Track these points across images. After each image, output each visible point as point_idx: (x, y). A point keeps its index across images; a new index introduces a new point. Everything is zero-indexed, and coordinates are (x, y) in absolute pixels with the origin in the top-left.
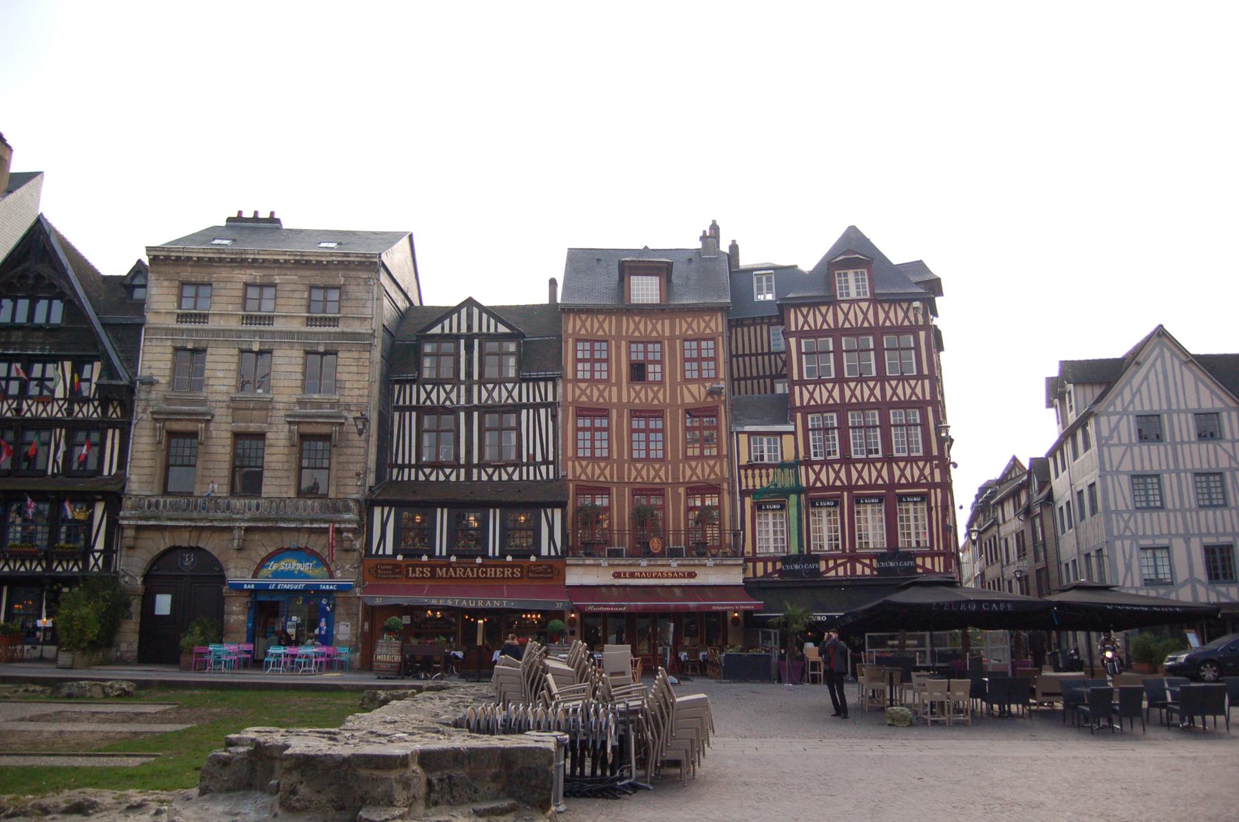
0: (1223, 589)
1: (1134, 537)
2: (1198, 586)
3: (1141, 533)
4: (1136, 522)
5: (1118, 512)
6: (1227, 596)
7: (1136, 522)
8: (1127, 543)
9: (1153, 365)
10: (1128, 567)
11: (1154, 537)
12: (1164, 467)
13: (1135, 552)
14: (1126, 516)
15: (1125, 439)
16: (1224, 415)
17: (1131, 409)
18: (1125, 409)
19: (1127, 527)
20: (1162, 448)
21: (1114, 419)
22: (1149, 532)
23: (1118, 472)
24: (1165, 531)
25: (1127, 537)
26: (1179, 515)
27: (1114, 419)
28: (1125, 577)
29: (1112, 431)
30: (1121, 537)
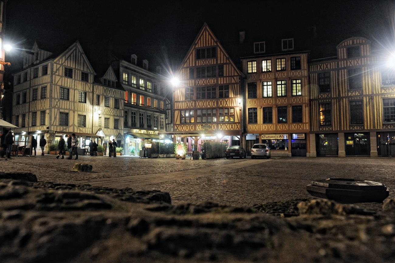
0: (81, 129)
1: (59, 108)
2: (75, 127)
3: (61, 107)
4: (60, 103)
5: (55, 99)
6: (82, 131)
7: (60, 103)
8: (56, 110)
9: (73, 52)
10: (55, 118)
11: (64, 109)
12: (71, 87)
13: (58, 113)
14: (57, 100)
15: (60, 74)
16: (89, 75)
17: (64, 64)
18: (62, 64)
19: (56, 104)
20: (71, 80)
21: (58, 66)
22: (63, 107)
23: (56, 85)
24: (68, 108)
25: (56, 108)
26: (73, 103)
27: (58, 66)
28: (54, 122)
29: (57, 70)
30: (55, 107)
